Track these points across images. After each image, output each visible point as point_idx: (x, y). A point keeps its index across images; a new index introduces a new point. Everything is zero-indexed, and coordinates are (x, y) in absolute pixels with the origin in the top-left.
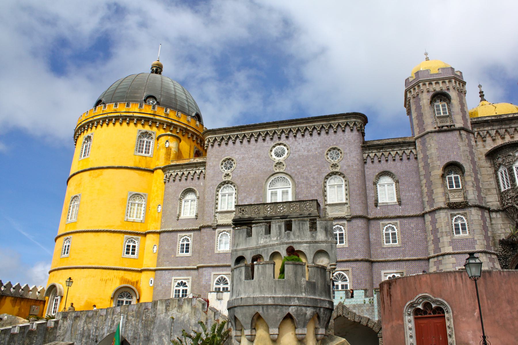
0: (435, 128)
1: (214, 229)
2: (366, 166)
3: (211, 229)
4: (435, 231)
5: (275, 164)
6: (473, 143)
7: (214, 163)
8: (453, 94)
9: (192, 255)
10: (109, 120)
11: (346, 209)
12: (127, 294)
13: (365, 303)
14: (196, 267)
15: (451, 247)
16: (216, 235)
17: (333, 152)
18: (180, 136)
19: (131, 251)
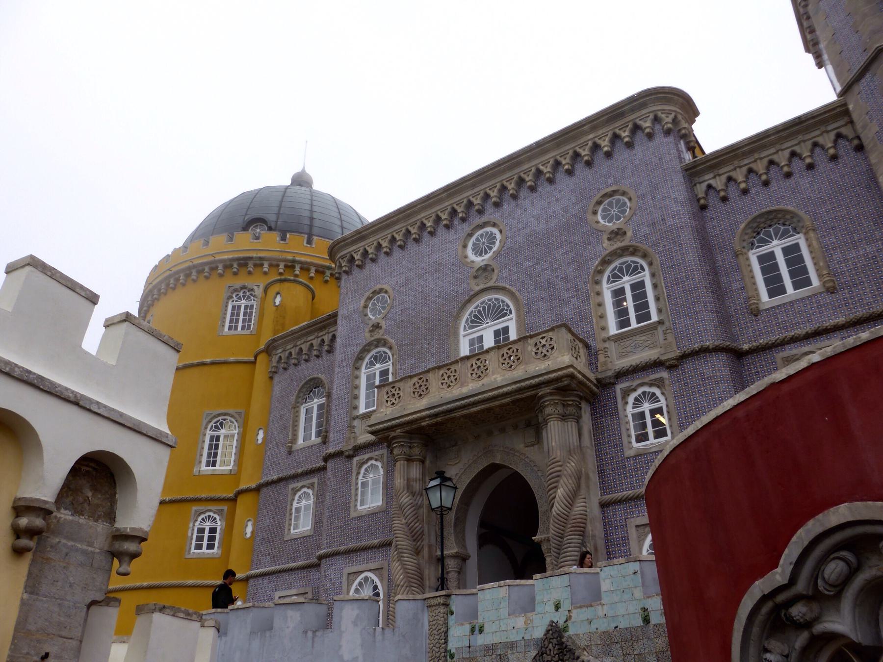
1: (350, 457)
2: (708, 214)
3: (343, 459)
5: (473, 272)
11: (661, 338)
13: (646, 620)
16: (354, 474)
17: (610, 204)
19: (205, 543)
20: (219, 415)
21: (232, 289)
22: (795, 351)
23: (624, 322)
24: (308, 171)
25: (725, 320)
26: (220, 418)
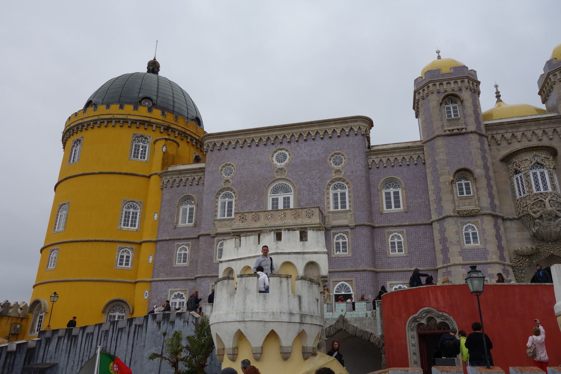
0: (445, 131)
1: (213, 237)
2: (371, 171)
4: (444, 240)
5: (276, 170)
6: (486, 147)
7: (214, 169)
8: (466, 95)
9: (190, 265)
10: (101, 123)
11: (349, 216)
12: (119, 309)
13: (367, 316)
14: (193, 278)
15: (461, 258)
16: (215, 244)
18: (178, 140)
19: (124, 262)
20: (130, 201)
21: (135, 136)
22: (391, 230)
23: (336, 207)
24: (157, 60)
25: (371, 214)
26: (130, 203)
